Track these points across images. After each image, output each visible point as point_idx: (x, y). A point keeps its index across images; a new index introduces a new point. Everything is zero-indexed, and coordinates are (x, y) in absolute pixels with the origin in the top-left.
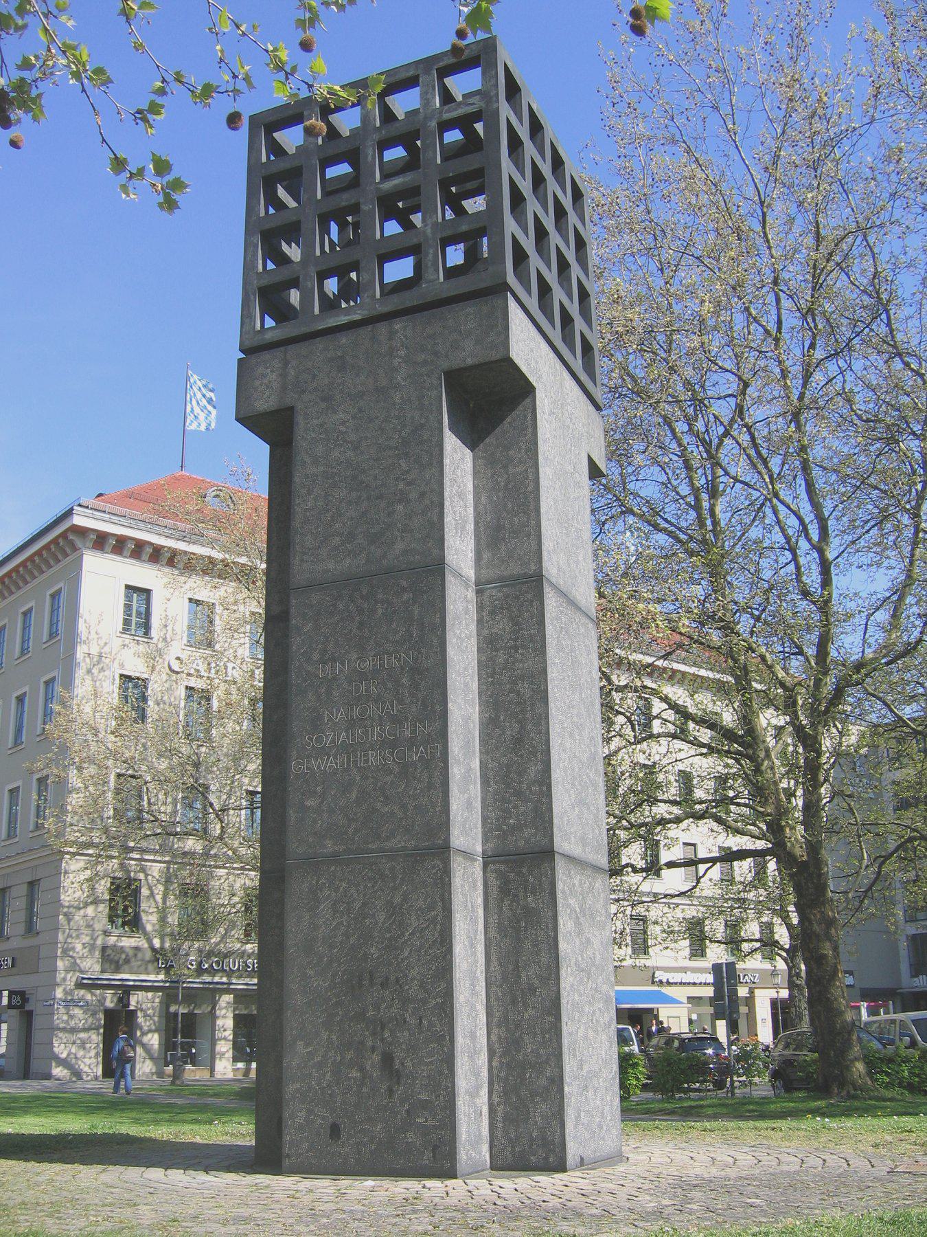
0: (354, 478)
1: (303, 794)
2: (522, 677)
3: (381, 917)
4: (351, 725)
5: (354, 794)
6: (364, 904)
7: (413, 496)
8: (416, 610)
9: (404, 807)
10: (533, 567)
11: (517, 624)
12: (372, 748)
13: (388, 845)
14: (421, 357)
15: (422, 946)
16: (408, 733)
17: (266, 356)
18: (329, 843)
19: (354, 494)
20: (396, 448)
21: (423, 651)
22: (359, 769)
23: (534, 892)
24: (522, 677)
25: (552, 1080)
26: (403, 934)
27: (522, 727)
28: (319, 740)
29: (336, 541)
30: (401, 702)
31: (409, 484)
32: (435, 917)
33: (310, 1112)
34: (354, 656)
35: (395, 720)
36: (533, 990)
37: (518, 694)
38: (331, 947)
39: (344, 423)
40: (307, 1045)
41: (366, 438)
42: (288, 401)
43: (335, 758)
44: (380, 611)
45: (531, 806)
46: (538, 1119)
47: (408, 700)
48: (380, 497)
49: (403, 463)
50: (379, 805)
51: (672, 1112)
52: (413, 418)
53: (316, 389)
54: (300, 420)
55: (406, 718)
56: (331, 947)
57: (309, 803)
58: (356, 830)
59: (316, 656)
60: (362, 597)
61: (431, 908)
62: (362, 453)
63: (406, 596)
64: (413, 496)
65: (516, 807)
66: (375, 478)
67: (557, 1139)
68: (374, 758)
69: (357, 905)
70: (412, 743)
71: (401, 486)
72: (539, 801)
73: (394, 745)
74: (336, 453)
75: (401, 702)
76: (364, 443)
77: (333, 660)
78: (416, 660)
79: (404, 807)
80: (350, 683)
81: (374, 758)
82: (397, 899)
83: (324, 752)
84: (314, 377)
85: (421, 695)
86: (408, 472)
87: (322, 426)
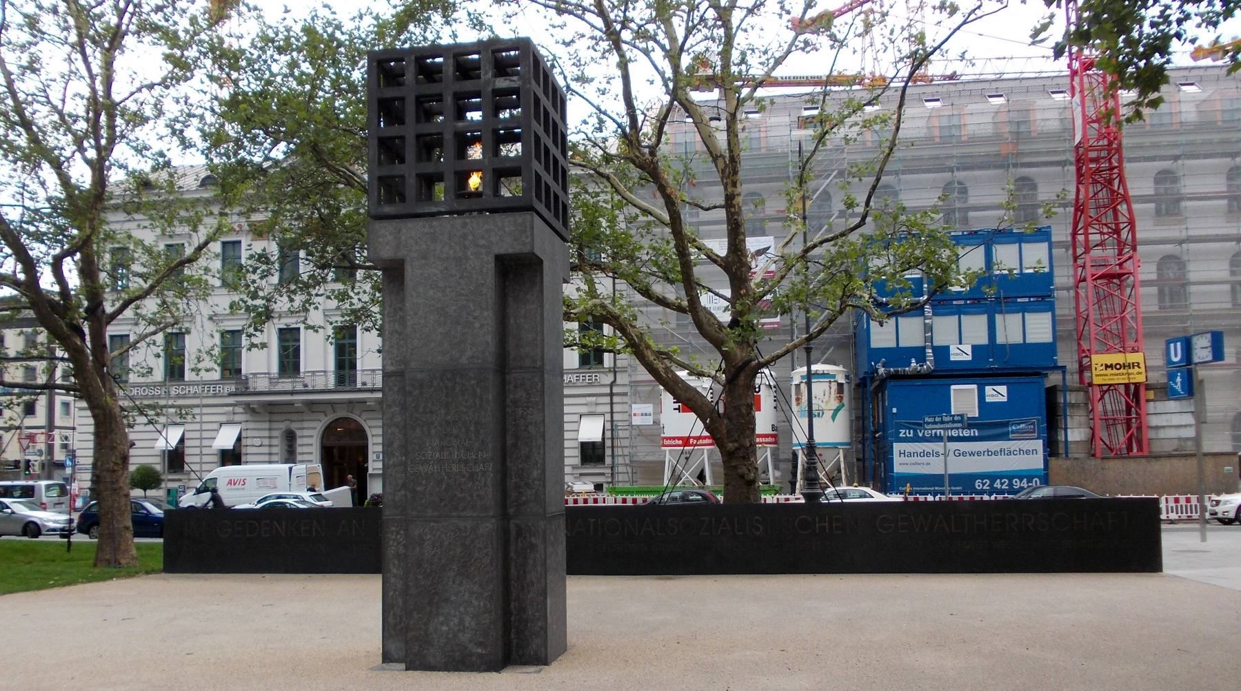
3: (459, 550)
4: (442, 449)
7: (477, 325)
8: (478, 390)
9: (471, 496)
10: (539, 364)
11: (528, 394)
13: (463, 514)
14: (482, 242)
17: (385, 223)
25: (541, 628)
28: (424, 455)
34: (443, 411)
35: (468, 450)
42: (400, 255)
54: (408, 268)
64: (477, 325)
68: (455, 468)
71: (470, 318)
73: (466, 462)
74: (431, 292)
81: (455, 468)
82: (468, 542)
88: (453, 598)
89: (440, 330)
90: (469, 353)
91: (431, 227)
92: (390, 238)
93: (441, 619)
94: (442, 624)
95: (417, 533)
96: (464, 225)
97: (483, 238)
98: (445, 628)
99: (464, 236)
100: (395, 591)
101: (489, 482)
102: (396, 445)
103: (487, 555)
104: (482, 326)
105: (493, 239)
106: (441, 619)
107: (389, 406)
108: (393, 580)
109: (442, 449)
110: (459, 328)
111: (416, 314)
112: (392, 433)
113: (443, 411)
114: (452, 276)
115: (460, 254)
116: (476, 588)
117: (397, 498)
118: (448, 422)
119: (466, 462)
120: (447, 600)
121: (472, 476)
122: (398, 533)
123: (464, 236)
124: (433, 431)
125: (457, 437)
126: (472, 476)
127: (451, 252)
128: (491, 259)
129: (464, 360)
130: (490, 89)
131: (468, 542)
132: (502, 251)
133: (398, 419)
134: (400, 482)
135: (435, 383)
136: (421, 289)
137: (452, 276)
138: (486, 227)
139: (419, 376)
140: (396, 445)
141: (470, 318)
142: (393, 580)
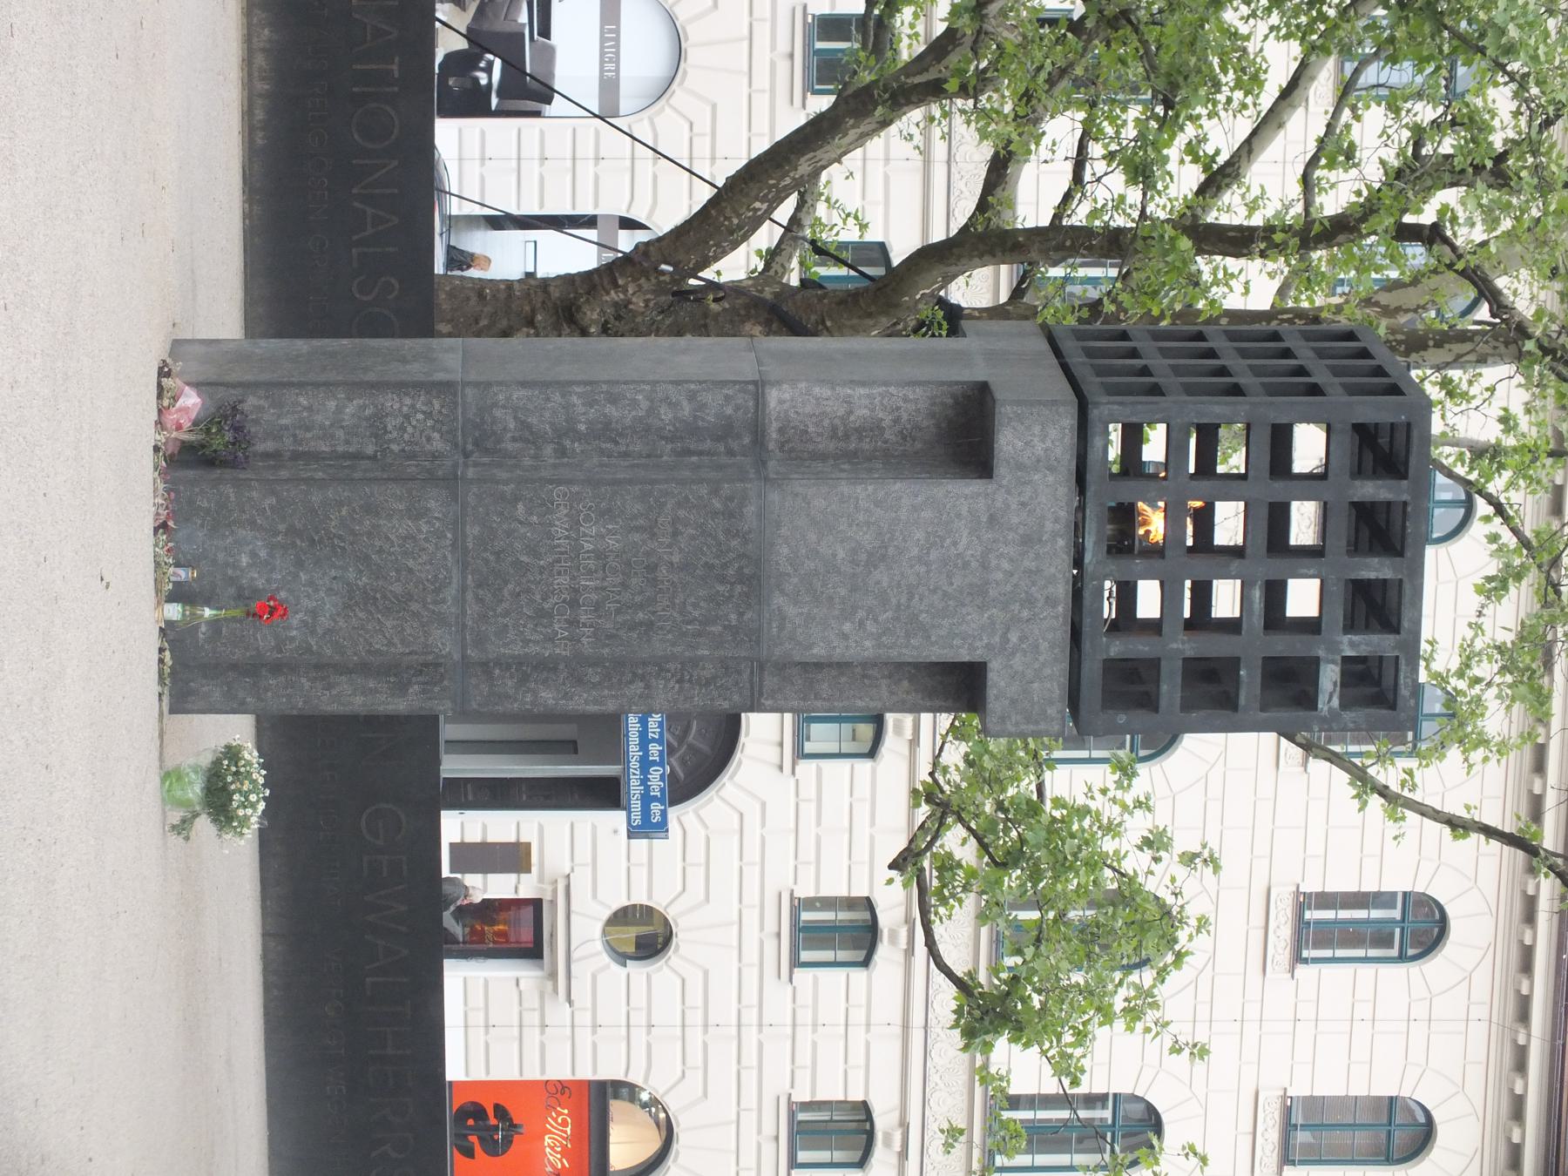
0: (883, 558)
1: (531, 500)
2: (648, 687)
3: (397, 588)
5: (525, 559)
6: (410, 571)
7: (847, 627)
8: (716, 629)
9: (506, 614)
12: (573, 578)
13: (469, 596)
14: (1014, 638)
15: (367, 631)
16: (583, 618)
17: (1070, 439)
18: (476, 530)
19: (864, 557)
20: (908, 607)
21: (670, 636)
22: (552, 564)
23: (424, 692)
24: (648, 687)
25: (243, 703)
26: (379, 611)
27: (594, 686)
28: (588, 519)
29: (812, 537)
30: (618, 612)
31: (861, 623)
32: (394, 645)
33: (208, 511)
34: (676, 559)
35: (598, 606)
36: (329, 687)
37: (631, 682)
38: (369, 534)
39: (955, 544)
40: (272, 507)
41: (928, 572)
42: (1001, 470)
43: (567, 537)
44: (721, 588)
45: (511, 692)
46: (205, 689)
47: (620, 619)
48: (854, 589)
49: (889, 614)
50: (510, 586)
51: (250, 75)
52: (940, 627)
53: (1008, 506)
54: (974, 486)
55: (600, 617)
56: (369, 534)
57: (520, 506)
58: (487, 561)
59: (682, 513)
60: (741, 568)
61: (403, 641)
62: (912, 567)
63: (733, 617)
64: (847, 627)
65: (512, 677)
66: (878, 583)
67: (189, 706)
69: (411, 563)
70: (573, 623)
72: (516, 700)
74: (919, 535)
75: (618, 612)
76: (923, 569)
77: (675, 534)
78: (661, 628)
79: (506, 614)
80: (648, 554)
82: (415, 607)
83: (575, 524)
84: (1023, 504)
85: (621, 633)
86: (876, 621)
87: (959, 516)
88: (303, 577)
89: (841, 554)
90: (791, 611)
91: (1055, 535)
92: (1039, 448)
93: (263, 554)
94: (254, 555)
95: (432, 504)
96: (1051, 601)
97: (1022, 639)
98: (245, 560)
99: (1029, 602)
100: (310, 409)
101: (533, 649)
102: (611, 410)
103: (390, 643)
104: (845, 637)
105: (1017, 662)
106: (263, 554)
107: (692, 397)
108: (332, 404)
109: (600, 555)
110: (843, 592)
111: (877, 504)
112: (634, 403)
113: (676, 559)
114: (950, 576)
115: (992, 593)
116: (324, 621)
117: (498, 413)
118: (652, 568)
119: (574, 604)
120: (299, 564)
121: (542, 615)
122: (428, 415)
123: (1029, 602)
124: (636, 537)
125: (624, 585)
126: (542, 615)
127: (999, 576)
128: (976, 657)
129: (778, 600)
130: (1321, 653)
131: (415, 607)
132: (992, 676)
133: (666, 414)
134: (533, 420)
135: (734, 543)
136: (927, 514)
137: (950, 576)
138: (1044, 645)
139: (750, 510)
140: (611, 410)
141: (861, 614)
142: (332, 404)
